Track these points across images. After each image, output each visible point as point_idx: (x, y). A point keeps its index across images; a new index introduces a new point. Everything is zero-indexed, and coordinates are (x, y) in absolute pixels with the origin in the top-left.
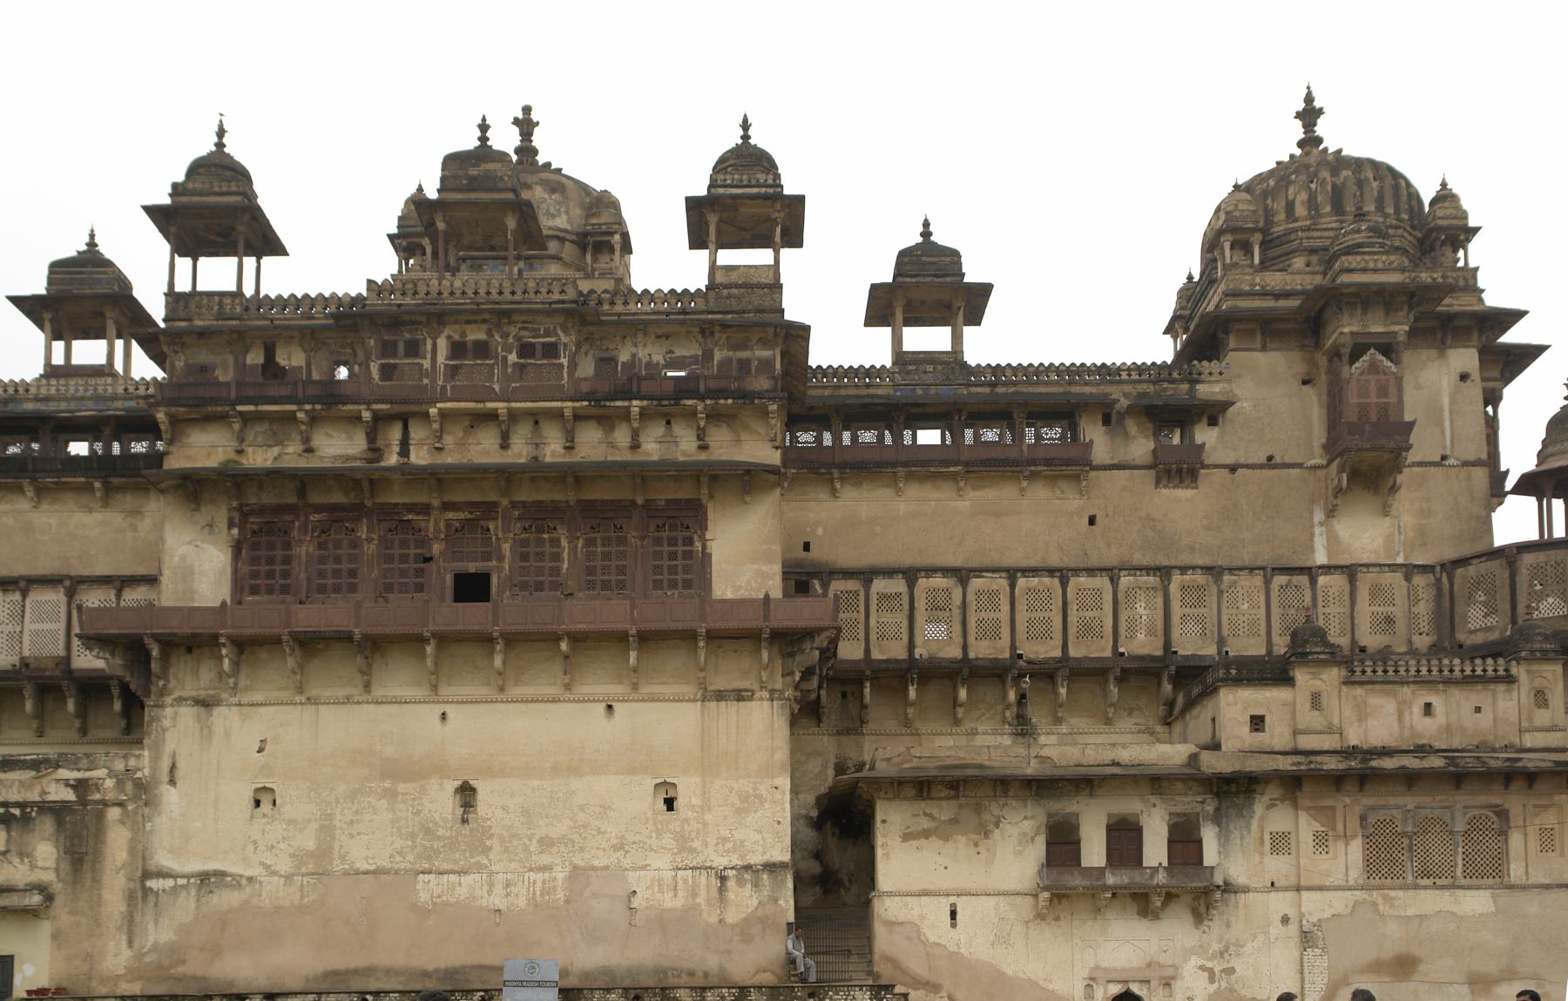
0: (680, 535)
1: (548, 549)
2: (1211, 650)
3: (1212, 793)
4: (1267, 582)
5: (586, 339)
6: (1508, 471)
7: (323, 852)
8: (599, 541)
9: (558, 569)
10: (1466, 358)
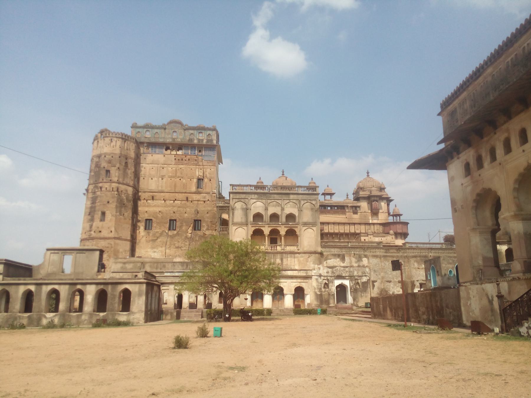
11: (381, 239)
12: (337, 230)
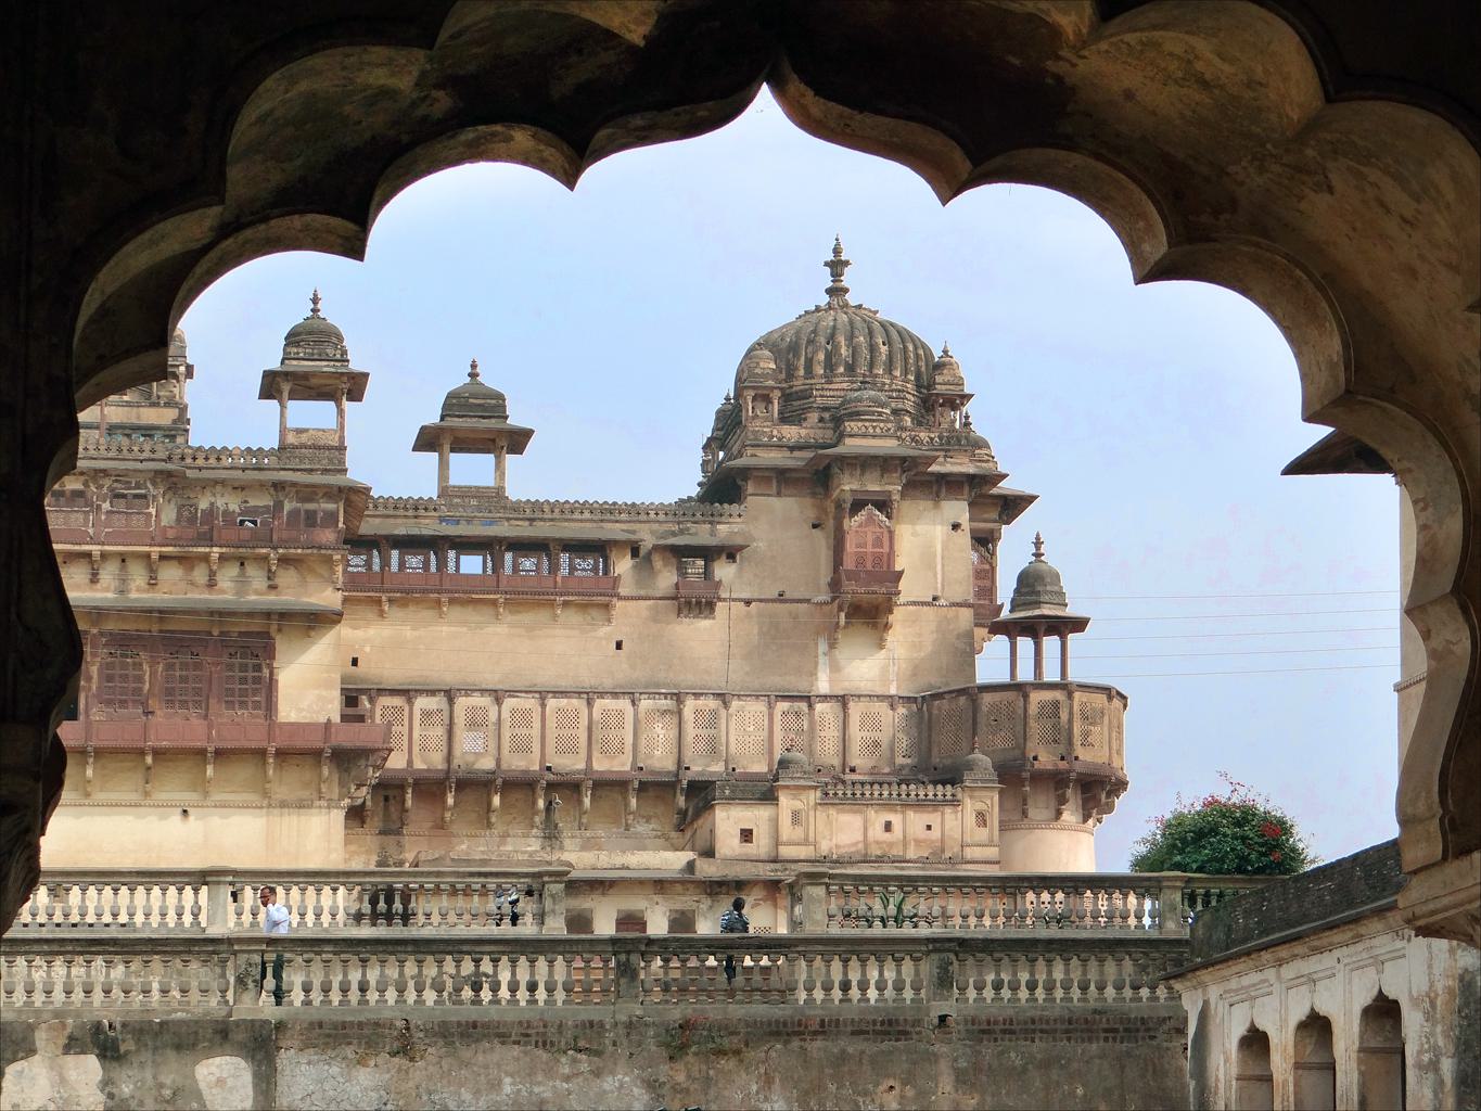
0: (251, 662)
1: (131, 672)
2: (718, 768)
3: (706, 893)
4: (771, 707)
5: (170, 488)
6: (1003, 604)
8: (177, 666)
9: (141, 689)
10: (958, 510)
11: (888, 827)
12: (529, 750)
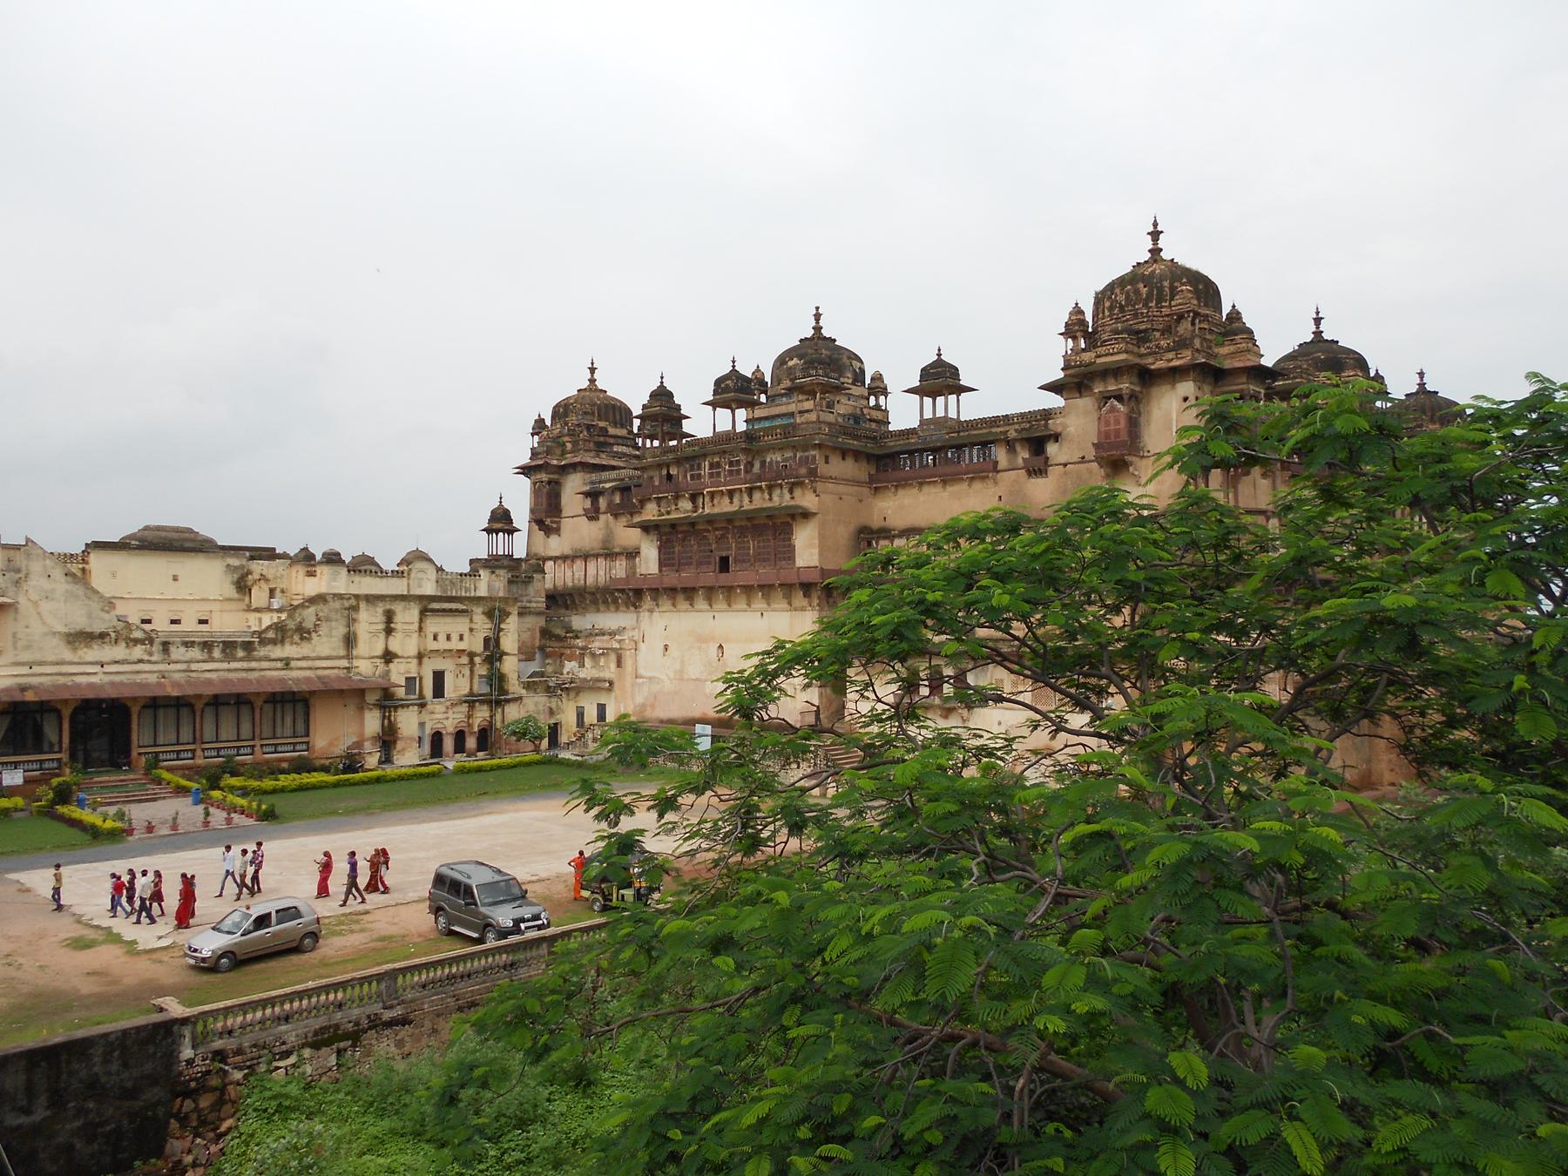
7: (682, 671)
